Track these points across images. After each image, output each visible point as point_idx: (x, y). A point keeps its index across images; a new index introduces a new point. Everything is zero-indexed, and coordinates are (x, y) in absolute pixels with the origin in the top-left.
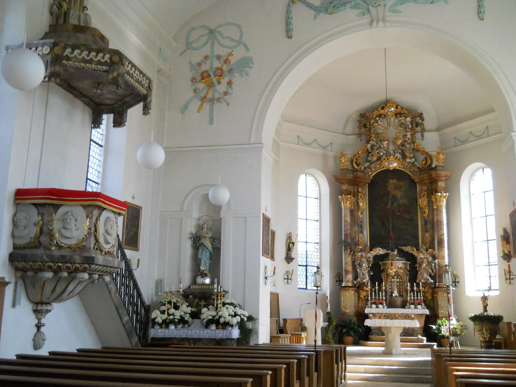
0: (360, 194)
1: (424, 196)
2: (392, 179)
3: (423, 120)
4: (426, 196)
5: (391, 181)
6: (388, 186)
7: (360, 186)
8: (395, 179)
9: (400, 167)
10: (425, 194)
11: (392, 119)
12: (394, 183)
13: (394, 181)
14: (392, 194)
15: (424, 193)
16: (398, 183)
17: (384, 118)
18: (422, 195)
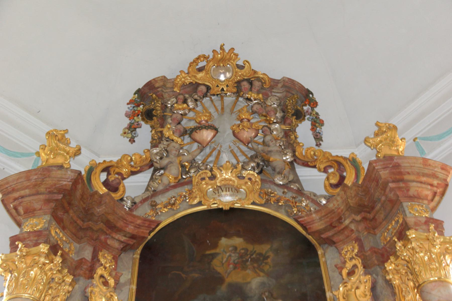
0: (100, 271)
1: (351, 273)
2: (227, 235)
3: (314, 104)
4: (360, 270)
5: (224, 241)
6: (214, 256)
7: (106, 246)
8: (239, 236)
9: (254, 203)
10: (355, 266)
11: (229, 100)
12: (235, 248)
13: (238, 241)
14: (228, 280)
15: (349, 265)
16: (250, 247)
17: (205, 95)
18: (345, 272)
